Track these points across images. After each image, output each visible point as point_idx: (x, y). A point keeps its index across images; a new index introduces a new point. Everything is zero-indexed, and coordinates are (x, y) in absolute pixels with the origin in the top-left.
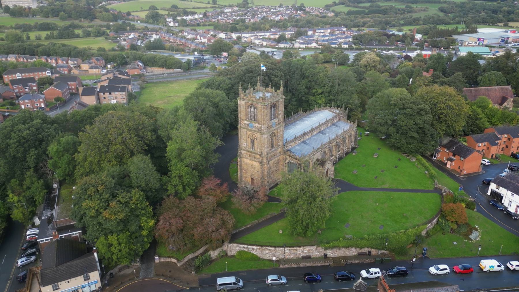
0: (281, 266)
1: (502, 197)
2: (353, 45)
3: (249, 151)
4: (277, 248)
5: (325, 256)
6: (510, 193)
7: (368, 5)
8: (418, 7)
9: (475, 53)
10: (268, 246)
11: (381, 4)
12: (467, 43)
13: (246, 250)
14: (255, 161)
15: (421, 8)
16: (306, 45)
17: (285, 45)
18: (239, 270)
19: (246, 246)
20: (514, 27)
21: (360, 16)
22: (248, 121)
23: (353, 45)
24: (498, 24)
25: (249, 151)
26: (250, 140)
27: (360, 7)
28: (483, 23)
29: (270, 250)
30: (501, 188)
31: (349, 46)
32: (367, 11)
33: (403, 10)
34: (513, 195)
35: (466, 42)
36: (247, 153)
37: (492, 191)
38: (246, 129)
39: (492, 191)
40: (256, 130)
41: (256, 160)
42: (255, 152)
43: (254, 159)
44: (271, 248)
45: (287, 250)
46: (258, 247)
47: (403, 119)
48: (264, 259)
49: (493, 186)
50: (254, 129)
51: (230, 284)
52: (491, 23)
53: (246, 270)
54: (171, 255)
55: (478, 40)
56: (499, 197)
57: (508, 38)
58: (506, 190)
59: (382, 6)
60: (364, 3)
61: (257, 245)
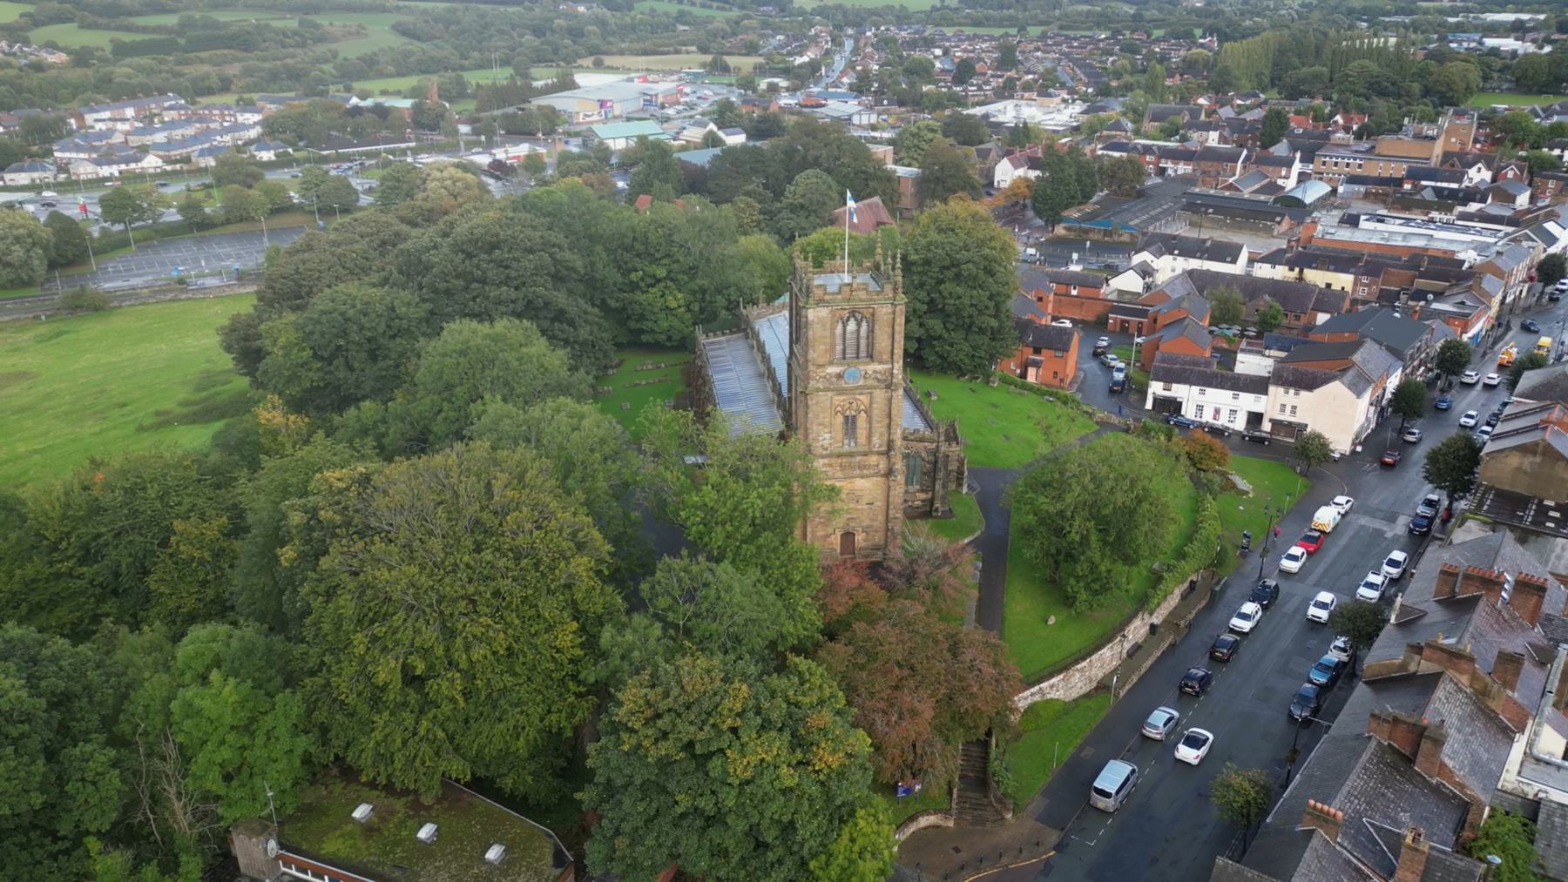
0: (1122, 693)
1: (1181, 403)
2: (290, 150)
3: (839, 456)
4: (1095, 657)
5: (1153, 628)
6: (1196, 389)
7: (171, 20)
8: (337, 23)
9: (651, 138)
10: (1077, 662)
11: (222, 17)
12: (581, 116)
13: (1037, 698)
14: (862, 477)
15: (344, 26)
16: (123, 167)
17: (36, 175)
18: (1071, 750)
19: (1037, 688)
20: (618, 68)
21: (171, 58)
22: (838, 365)
23: (290, 150)
24: (580, 62)
25: (839, 456)
26: (840, 419)
27: (145, 30)
28: (540, 62)
29: (1082, 669)
30: (1175, 386)
31: (276, 155)
32: (182, 41)
33: (295, 33)
34: (1202, 392)
35: (578, 113)
36: (833, 461)
37: (1156, 400)
38: (832, 390)
39: (1156, 400)
40: (871, 382)
41: (865, 472)
42: (861, 449)
43: (857, 472)
44: (1084, 664)
45: (1106, 652)
46: (1061, 676)
47: (960, 290)
48: (1076, 700)
49: (1156, 388)
50: (861, 382)
51: (1127, 779)
52: (564, 60)
53: (1079, 741)
54: (911, 812)
55: (601, 106)
56: (1174, 406)
57: (656, 95)
58: (1187, 386)
59: (226, 25)
60: (139, 14)
61: (1059, 672)
